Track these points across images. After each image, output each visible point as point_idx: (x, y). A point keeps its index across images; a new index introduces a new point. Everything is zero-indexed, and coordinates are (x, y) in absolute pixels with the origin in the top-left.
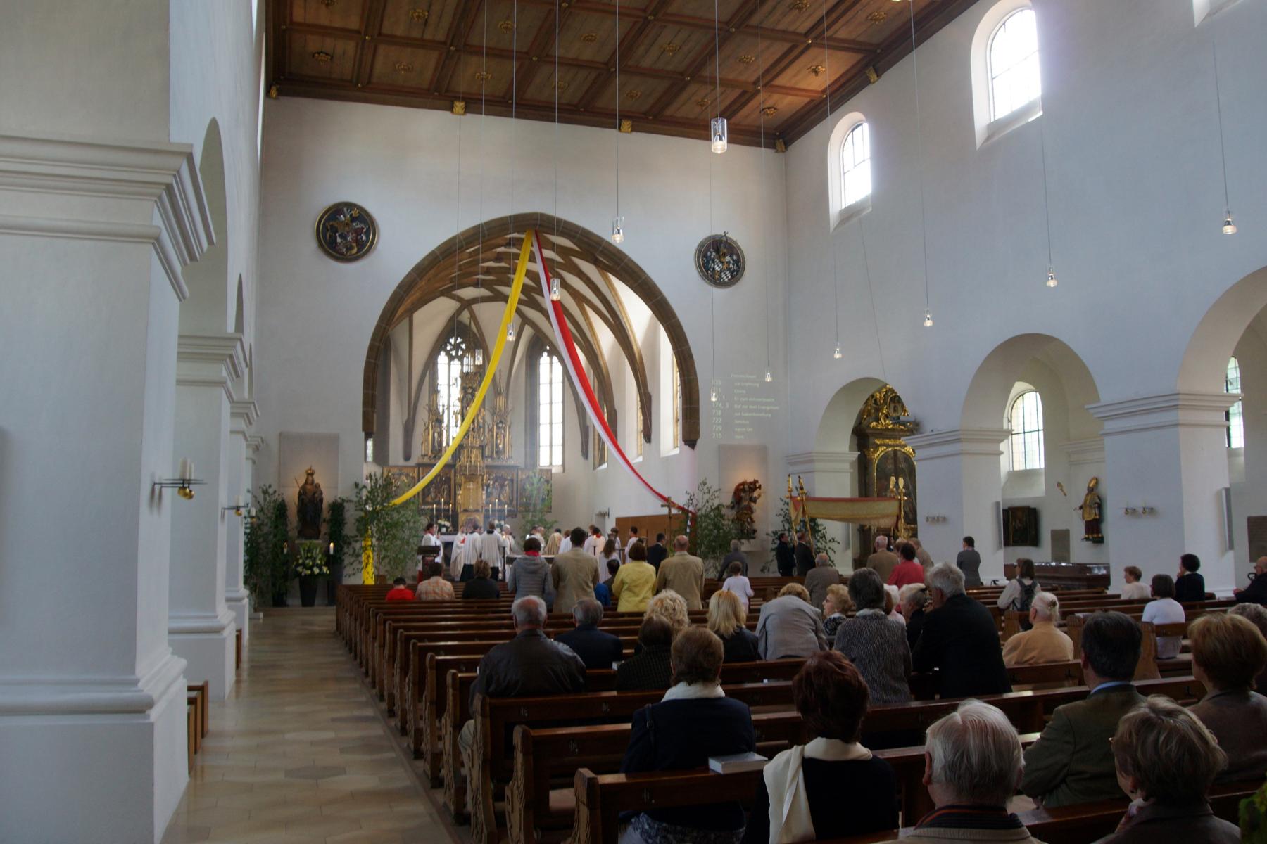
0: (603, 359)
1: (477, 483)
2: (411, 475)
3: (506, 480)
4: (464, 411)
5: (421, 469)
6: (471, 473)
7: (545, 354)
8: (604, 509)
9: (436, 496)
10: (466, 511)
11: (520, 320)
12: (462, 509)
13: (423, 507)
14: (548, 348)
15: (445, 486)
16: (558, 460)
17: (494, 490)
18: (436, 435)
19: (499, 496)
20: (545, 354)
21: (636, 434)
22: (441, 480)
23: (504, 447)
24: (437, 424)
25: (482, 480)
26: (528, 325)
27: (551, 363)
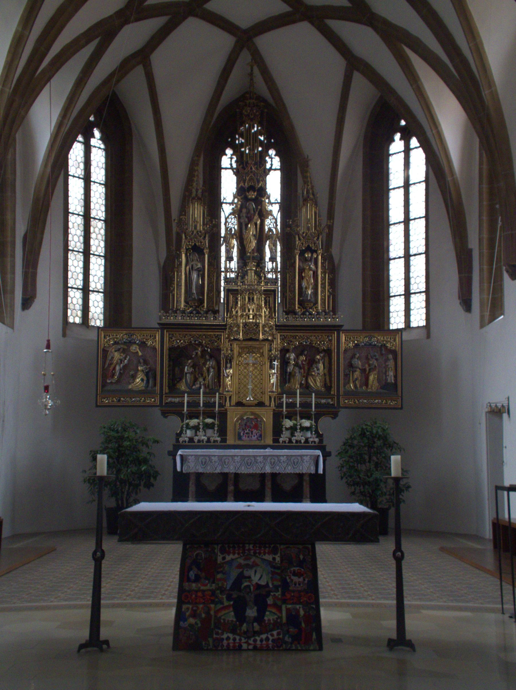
0: (491, 83)
1: (262, 355)
2: (149, 343)
3: (318, 352)
4: (244, 230)
6: (249, 336)
7: (398, 136)
9: (196, 380)
10: (239, 404)
12: (233, 402)
13: (169, 400)
14: (403, 123)
15: (211, 363)
17: (297, 370)
18: (195, 276)
19: (307, 380)
20: (398, 136)
22: (204, 351)
25: (270, 350)
26: (358, 70)
27: (407, 151)
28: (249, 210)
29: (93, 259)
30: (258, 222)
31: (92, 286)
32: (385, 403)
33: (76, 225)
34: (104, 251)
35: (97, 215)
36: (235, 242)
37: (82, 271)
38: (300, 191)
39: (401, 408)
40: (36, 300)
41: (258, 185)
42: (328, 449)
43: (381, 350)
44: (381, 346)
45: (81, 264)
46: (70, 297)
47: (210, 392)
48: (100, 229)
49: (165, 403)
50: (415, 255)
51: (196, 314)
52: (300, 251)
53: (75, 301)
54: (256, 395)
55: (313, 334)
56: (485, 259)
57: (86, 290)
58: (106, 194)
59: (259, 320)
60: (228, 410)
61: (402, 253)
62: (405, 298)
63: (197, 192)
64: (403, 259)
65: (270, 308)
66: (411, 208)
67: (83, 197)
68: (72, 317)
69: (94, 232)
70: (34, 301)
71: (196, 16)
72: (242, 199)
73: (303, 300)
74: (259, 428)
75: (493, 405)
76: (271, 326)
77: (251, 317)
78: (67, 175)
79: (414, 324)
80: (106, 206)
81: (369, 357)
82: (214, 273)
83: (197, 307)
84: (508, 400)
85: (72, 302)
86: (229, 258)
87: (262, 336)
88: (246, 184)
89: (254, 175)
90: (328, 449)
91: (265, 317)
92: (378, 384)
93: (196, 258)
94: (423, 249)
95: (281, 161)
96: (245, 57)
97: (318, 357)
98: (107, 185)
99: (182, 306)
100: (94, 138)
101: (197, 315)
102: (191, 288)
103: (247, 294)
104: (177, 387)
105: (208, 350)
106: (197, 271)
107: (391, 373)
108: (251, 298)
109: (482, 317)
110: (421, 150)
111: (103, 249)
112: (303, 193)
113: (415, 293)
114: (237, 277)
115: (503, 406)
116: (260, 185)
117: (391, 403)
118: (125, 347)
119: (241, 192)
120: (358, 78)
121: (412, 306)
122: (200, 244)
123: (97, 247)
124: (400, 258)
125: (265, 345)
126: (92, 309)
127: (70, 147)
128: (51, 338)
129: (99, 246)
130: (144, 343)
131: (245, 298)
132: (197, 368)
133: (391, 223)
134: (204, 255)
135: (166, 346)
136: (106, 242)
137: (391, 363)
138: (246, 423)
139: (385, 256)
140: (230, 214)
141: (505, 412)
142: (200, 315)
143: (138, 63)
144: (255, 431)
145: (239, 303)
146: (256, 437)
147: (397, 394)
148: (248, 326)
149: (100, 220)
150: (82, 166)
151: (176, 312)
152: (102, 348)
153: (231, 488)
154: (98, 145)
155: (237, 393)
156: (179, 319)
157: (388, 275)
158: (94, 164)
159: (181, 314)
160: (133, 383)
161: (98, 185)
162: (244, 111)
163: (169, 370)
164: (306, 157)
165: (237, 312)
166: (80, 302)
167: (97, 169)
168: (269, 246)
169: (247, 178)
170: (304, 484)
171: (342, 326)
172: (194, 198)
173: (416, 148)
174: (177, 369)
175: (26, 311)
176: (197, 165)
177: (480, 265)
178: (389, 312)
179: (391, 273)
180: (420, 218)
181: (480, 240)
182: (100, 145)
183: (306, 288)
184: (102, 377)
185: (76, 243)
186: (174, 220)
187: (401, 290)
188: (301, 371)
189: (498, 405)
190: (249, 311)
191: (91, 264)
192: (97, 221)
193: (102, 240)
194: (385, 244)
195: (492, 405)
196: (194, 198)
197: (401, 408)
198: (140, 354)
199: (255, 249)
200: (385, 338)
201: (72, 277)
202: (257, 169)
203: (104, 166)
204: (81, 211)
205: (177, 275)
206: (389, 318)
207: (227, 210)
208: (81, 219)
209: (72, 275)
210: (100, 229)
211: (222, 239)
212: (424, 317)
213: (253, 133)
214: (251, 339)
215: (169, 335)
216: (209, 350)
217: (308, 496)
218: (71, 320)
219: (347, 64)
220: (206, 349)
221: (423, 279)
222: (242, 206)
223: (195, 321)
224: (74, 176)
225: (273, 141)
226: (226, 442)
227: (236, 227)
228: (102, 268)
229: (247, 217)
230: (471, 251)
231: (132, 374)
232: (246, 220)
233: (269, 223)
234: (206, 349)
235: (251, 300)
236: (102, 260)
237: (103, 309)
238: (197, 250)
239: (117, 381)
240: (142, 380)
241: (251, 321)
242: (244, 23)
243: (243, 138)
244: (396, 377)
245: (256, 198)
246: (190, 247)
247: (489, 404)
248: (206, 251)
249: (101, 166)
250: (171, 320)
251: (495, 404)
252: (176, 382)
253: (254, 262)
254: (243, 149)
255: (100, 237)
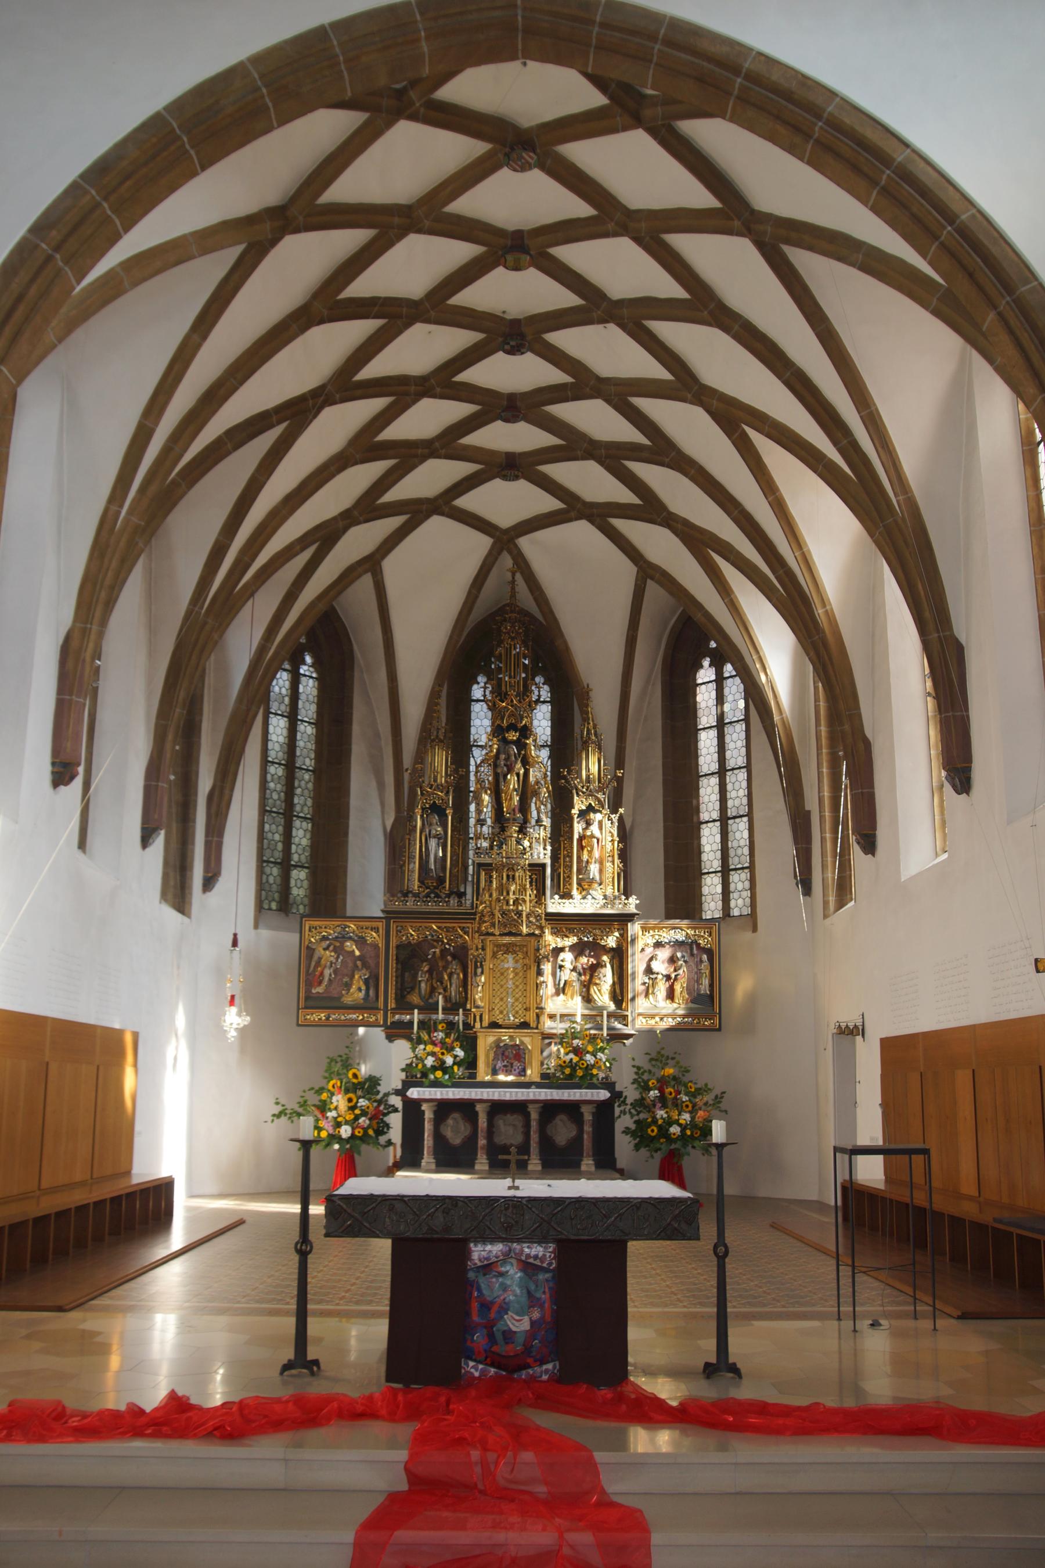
0: (824, 602)
5: (393, 926)
6: (507, 930)
7: (706, 662)
8: (849, 1017)
10: (494, 1025)
11: (635, 569)
12: (486, 1023)
13: (397, 1017)
14: (713, 645)
16: (739, 905)
18: (433, 843)
20: (706, 662)
21: (927, 794)
22: (444, 952)
23: (601, 871)
24: (436, 818)
26: (652, 579)
27: (720, 681)
28: (508, 754)
29: (297, 823)
30: (522, 772)
31: (295, 857)
32: (697, 1023)
33: (276, 776)
34: (311, 812)
35: (304, 764)
36: (486, 798)
37: (282, 840)
38: (577, 730)
39: (719, 1029)
40: (220, 879)
41: (521, 723)
42: (618, 1088)
43: (692, 949)
44: (692, 942)
45: (281, 828)
46: (265, 874)
47: (452, 1008)
48: (307, 783)
49: (391, 1023)
50: (734, 818)
51: (435, 897)
52: (579, 811)
53: (271, 880)
54: (517, 1012)
55: (597, 926)
56: (828, 826)
57: (286, 866)
58: (316, 736)
59: (521, 905)
60: (478, 1034)
61: (715, 815)
62: (723, 876)
63: (438, 732)
64: (718, 824)
65: (538, 890)
66: (728, 754)
67: (287, 742)
68: (267, 901)
69: (300, 787)
70: (218, 880)
71: (442, 514)
72: (498, 741)
73: (582, 880)
74: (522, 1059)
75: (843, 1025)
76: (539, 915)
77: (511, 902)
78: (267, 714)
79: (736, 912)
80: (316, 752)
81: (675, 959)
82: (459, 842)
83: (436, 888)
84: (863, 1018)
85: (267, 882)
86: (481, 822)
87: (526, 928)
88: (505, 721)
89: (516, 709)
90: (618, 1088)
91: (531, 901)
92: (687, 996)
93: (435, 821)
94: (744, 810)
95: (551, 691)
96: (506, 561)
97: (605, 958)
98: (318, 724)
99: (416, 888)
100: (305, 664)
101: (436, 899)
102: (427, 862)
103: (505, 870)
104: (408, 1000)
105: (449, 949)
106: (436, 839)
107: (706, 982)
108: (511, 876)
109: (826, 903)
110: (738, 680)
111: (311, 809)
112: (582, 733)
113: (736, 869)
114: (491, 847)
115: (856, 1026)
116: (524, 722)
117: (706, 1023)
118: (338, 944)
119: (498, 731)
120: (652, 589)
121: (732, 887)
122: (441, 801)
123: (302, 807)
124: (714, 821)
125: (530, 941)
126: (295, 891)
127: (274, 677)
128: (237, 932)
129: (305, 804)
130: (363, 938)
131: (503, 875)
132: (435, 973)
133: (701, 774)
134: (446, 816)
135: (393, 942)
136: (313, 798)
137: (705, 967)
138: (504, 1051)
139: (695, 819)
140: (482, 762)
141: (859, 1035)
142: (440, 899)
143: (366, 572)
144: (516, 1064)
145: (495, 883)
146: (517, 1071)
147: (714, 1010)
148: (506, 914)
149: (307, 770)
150: (287, 700)
151: (406, 895)
152: (306, 946)
153: (482, 1142)
154: (307, 673)
155: (490, 1009)
156: (410, 904)
157: (699, 845)
158: (303, 697)
159: (414, 899)
160: (347, 994)
161: (306, 724)
162: (502, 628)
163: (397, 977)
164: (586, 686)
165: (491, 896)
166: (279, 880)
167: (307, 704)
168: (536, 803)
169: (507, 714)
170: (585, 1136)
171: (638, 914)
172: (433, 741)
173: (731, 677)
174: (407, 974)
175: (208, 894)
176: (439, 697)
177: (821, 834)
178: (701, 895)
179: (704, 841)
180: (740, 768)
181: (821, 800)
182: (312, 672)
183: (588, 862)
184: (306, 985)
185: (275, 800)
186: (407, 770)
187: (717, 865)
188: (580, 978)
189: (849, 1024)
190: (508, 894)
191: (294, 830)
192: (304, 771)
193: (309, 797)
194: (694, 802)
195: (841, 1024)
196: (433, 741)
197: (719, 1029)
198: (357, 953)
199: (517, 811)
200: (697, 931)
201: (269, 848)
202: (520, 702)
203: (316, 701)
204: (284, 759)
205: (409, 844)
206: (701, 904)
207: (478, 755)
208: (283, 769)
209: (269, 844)
210: (307, 783)
211: (471, 794)
212: (748, 900)
213: (515, 655)
214: (510, 934)
215: (397, 927)
216: (452, 948)
217: (591, 1153)
218: (266, 906)
219: (638, 571)
220: (447, 946)
221: (746, 851)
222: (498, 750)
223: (431, 907)
224: (276, 714)
225: (540, 665)
226: (475, 1078)
227: (490, 779)
228: (308, 836)
229: (505, 765)
230: (809, 812)
231: (346, 982)
232: (505, 769)
233: (534, 775)
234: (447, 946)
235: (511, 878)
236: (308, 823)
237: (308, 891)
238: (437, 810)
239: (325, 990)
240: (360, 989)
241: (511, 907)
242: (505, 520)
243: (501, 663)
244: (711, 985)
245: (518, 739)
246: (427, 806)
247: (838, 1024)
248: (449, 812)
249: (312, 700)
250: (398, 905)
251: (845, 1024)
252: (406, 993)
253: (516, 826)
254: (501, 676)
255: (306, 792)
